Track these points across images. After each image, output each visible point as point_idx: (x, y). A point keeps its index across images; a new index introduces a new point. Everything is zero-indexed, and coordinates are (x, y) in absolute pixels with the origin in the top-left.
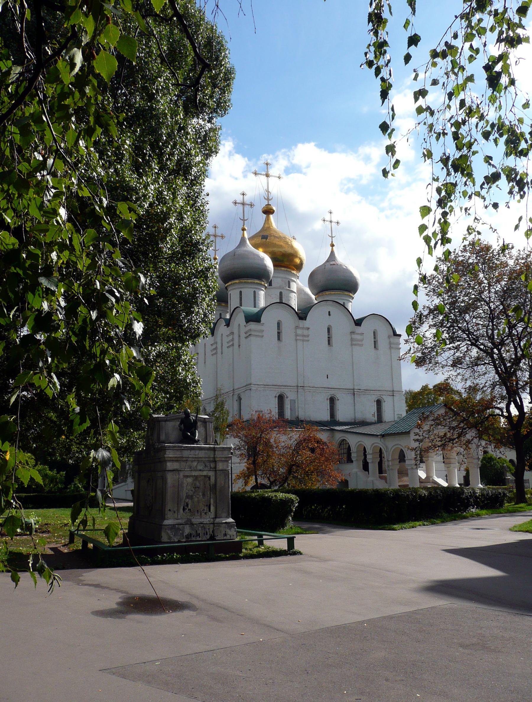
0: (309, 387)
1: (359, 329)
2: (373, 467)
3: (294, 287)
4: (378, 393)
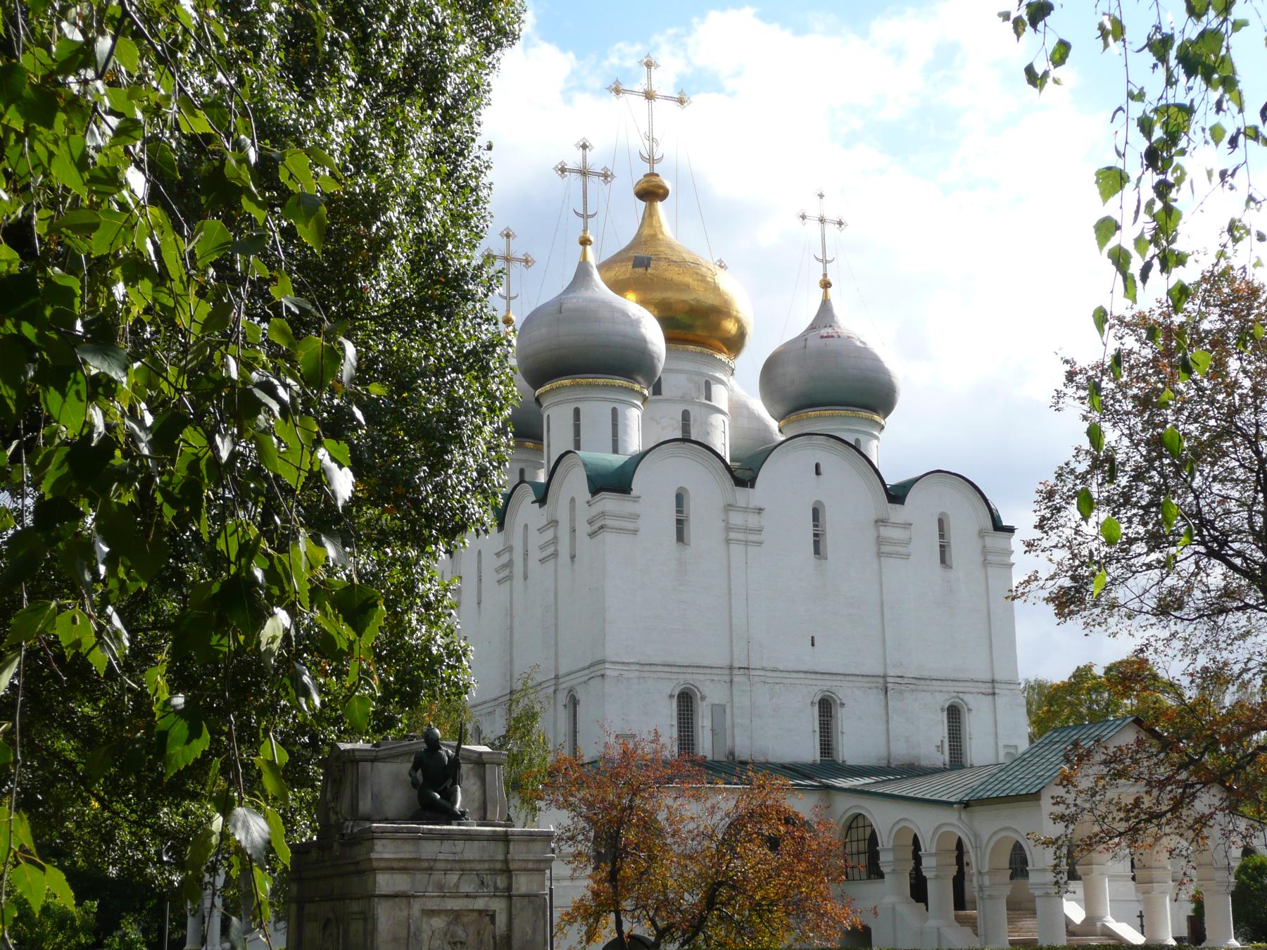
0: (763, 669)
1: (897, 513)
3: (721, 397)
4: (952, 687)
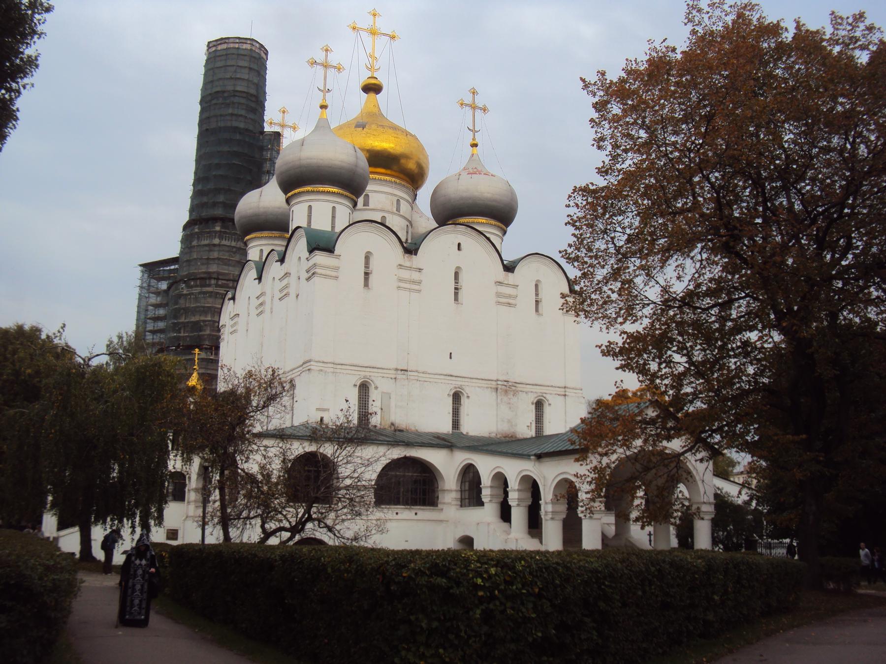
0: (417, 371)
1: (511, 278)
2: (519, 515)
4: (538, 389)
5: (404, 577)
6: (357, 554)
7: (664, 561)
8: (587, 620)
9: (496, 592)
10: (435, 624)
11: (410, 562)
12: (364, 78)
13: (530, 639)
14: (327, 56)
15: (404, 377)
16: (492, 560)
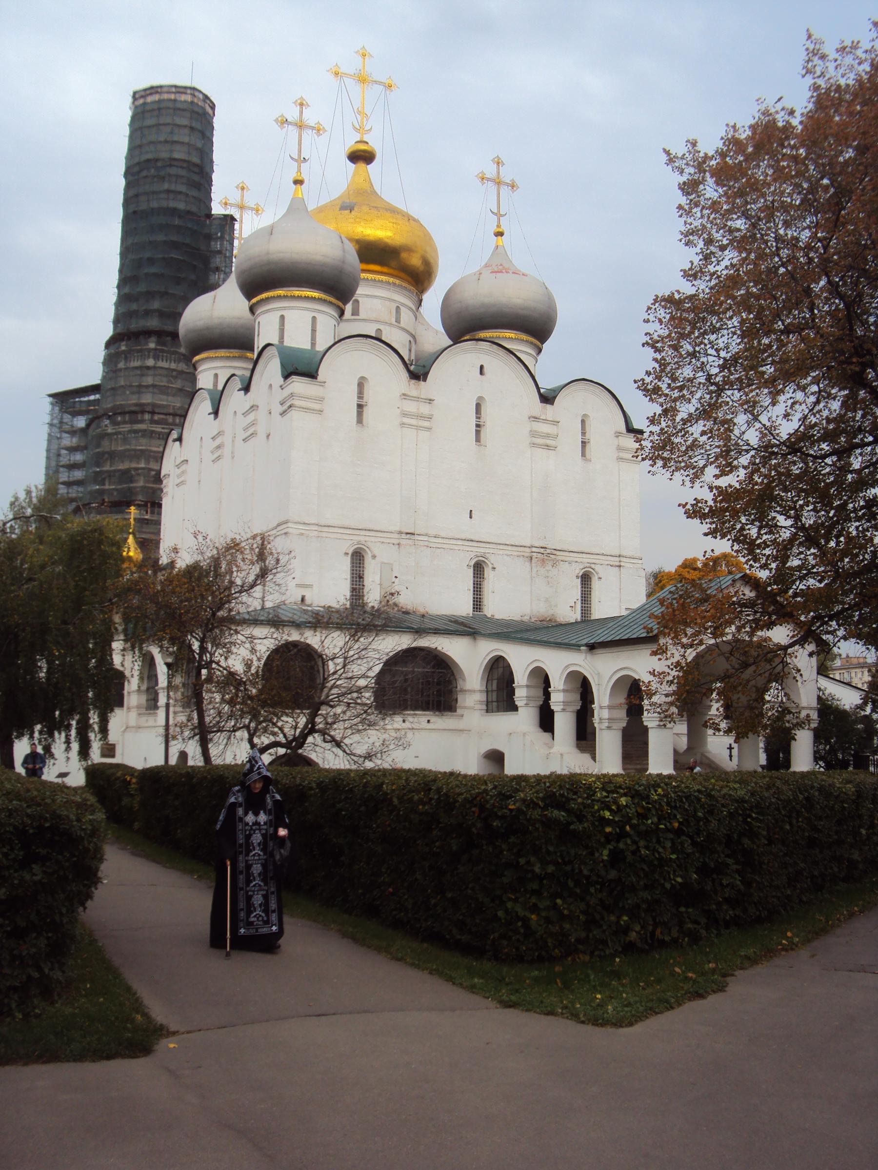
2: (564, 723)
4: (586, 559)
5: (511, 810)
6: (434, 781)
7: (812, 787)
8: (729, 861)
9: (628, 828)
10: (551, 869)
11: (517, 791)
12: (350, 142)
13: (668, 886)
14: (301, 113)
15: (410, 542)
16: (620, 787)
